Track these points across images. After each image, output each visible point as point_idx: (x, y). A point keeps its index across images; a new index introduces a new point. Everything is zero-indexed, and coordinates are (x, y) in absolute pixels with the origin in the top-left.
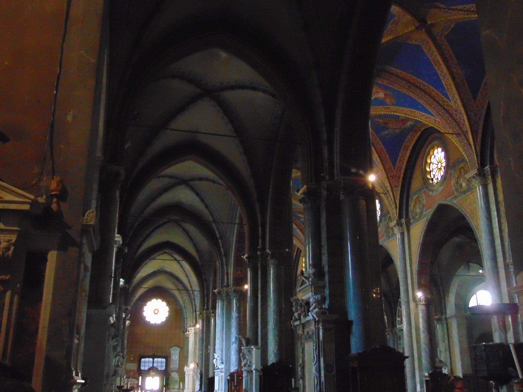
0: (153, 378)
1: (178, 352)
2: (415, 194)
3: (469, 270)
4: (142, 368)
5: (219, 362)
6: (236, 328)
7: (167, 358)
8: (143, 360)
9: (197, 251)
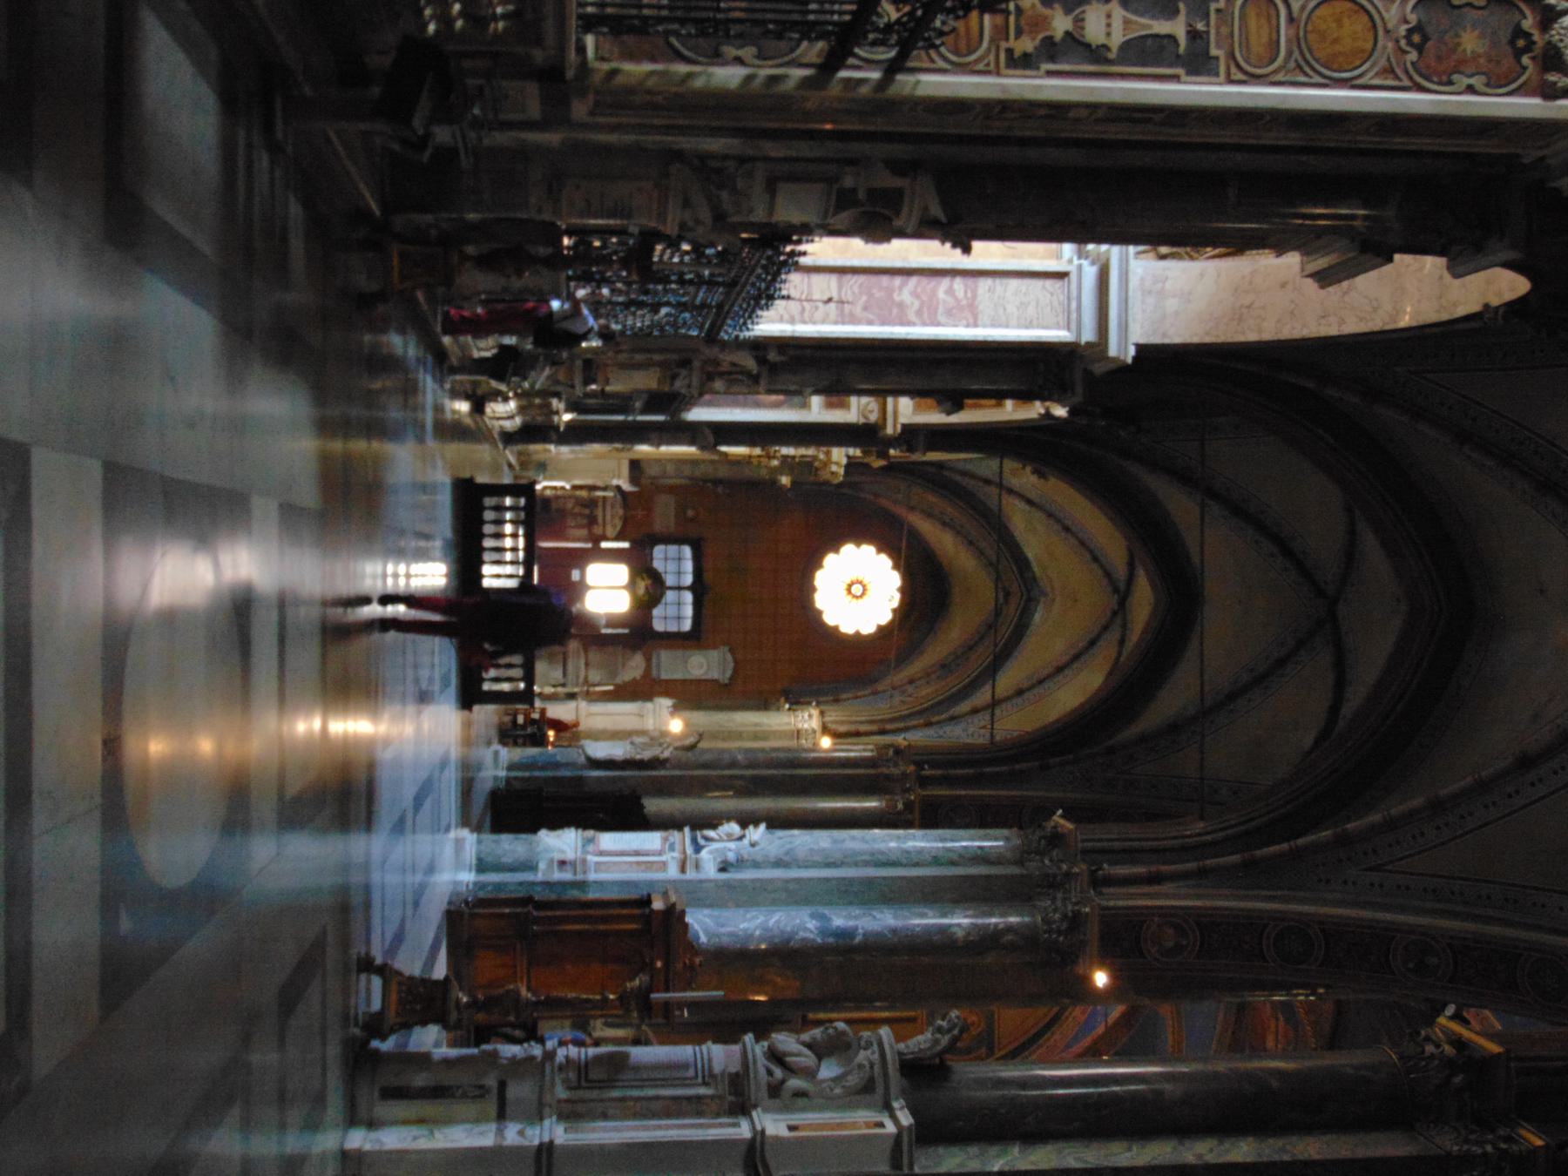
1: (715, 675)
4: (659, 551)
5: (731, 849)
6: (894, 931)
7: (692, 639)
8: (687, 551)
9: (1174, 728)
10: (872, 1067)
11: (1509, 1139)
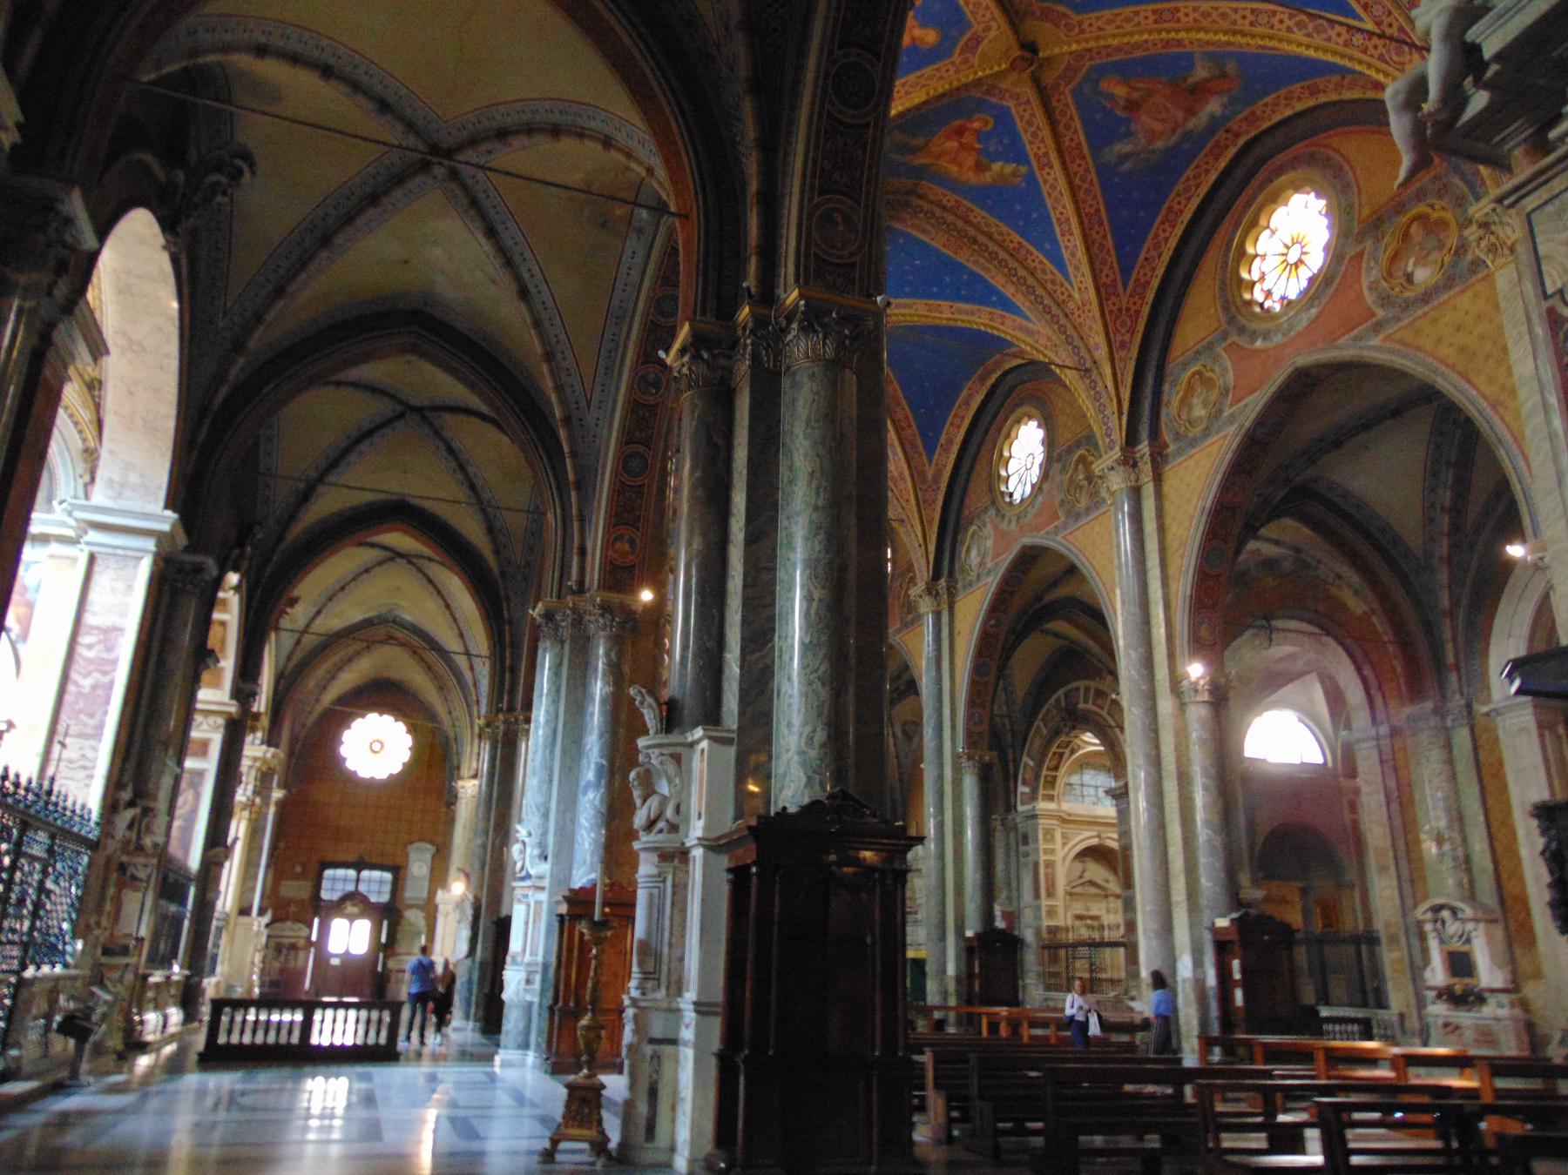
0: (351, 922)
1: (428, 857)
2: (1185, 366)
3: (1271, 640)
4: (325, 895)
5: (532, 851)
6: (601, 736)
7: (398, 871)
8: (328, 873)
9: (490, 530)
10: (662, 755)
11: (744, 329)
